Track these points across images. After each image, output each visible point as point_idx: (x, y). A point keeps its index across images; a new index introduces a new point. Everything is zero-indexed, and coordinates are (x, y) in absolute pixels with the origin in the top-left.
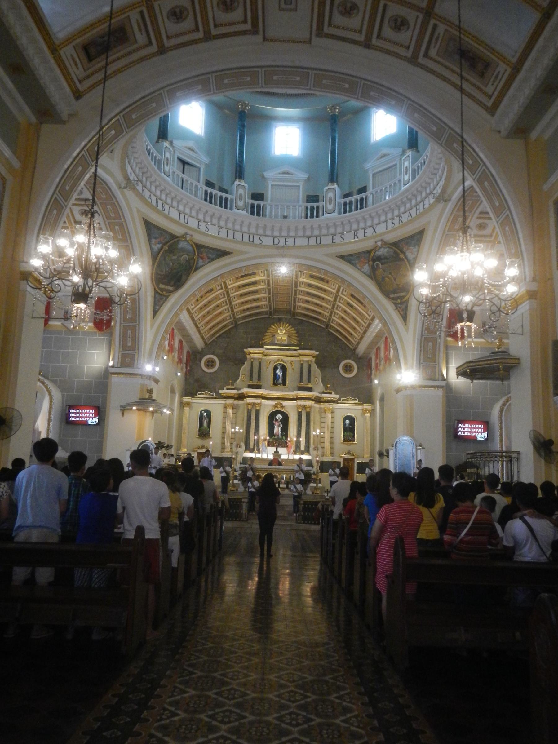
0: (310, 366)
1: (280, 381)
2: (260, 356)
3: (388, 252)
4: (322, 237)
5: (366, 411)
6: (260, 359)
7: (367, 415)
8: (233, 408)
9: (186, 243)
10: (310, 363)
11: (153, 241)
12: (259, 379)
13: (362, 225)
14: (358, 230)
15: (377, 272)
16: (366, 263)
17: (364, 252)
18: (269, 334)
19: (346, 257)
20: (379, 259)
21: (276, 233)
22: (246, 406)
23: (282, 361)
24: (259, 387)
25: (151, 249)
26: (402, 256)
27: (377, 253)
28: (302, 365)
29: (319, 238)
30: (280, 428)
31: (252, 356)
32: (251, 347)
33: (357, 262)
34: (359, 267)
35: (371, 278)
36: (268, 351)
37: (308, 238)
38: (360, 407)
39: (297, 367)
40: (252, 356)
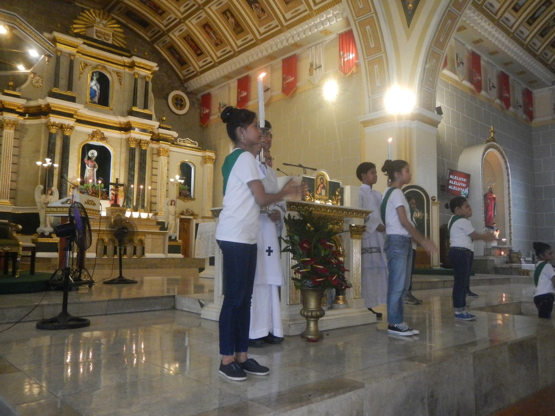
0: (147, 83)
1: (96, 99)
2: (73, 51)
5: (210, 158)
6: (70, 55)
7: (210, 165)
8: (16, 130)
10: (148, 79)
12: (70, 87)
18: (82, 22)
22: (43, 128)
23: (104, 67)
24: (72, 99)
28: (136, 80)
30: (96, 170)
31: (60, 46)
32: (57, 31)
36: (85, 46)
38: (200, 154)
39: (128, 82)
40: (60, 46)
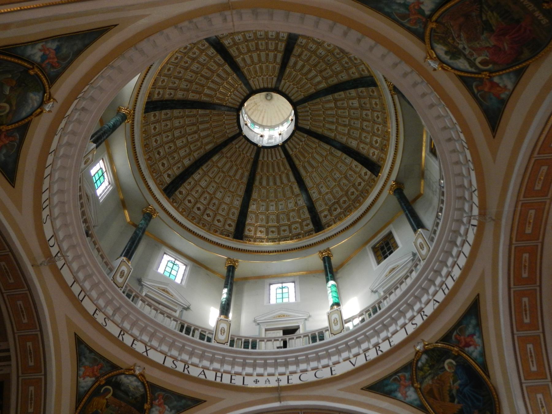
3: (137, 386)
4: (86, 297)
9: (36, 105)
11: (53, 46)
13: (136, 332)
14: (127, 333)
15: (96, 399)
16: (94, 375)
17: (108, 362)
19: (83, 346)
20: (117, 385)
21: (61, 235)
25: (34, 43)
26: (146, 406)
27: (123, 376)
29: (83, 294)
33: (87, 363)
34: (81, 373)
35: (79, 399)
37: (76, 280)
